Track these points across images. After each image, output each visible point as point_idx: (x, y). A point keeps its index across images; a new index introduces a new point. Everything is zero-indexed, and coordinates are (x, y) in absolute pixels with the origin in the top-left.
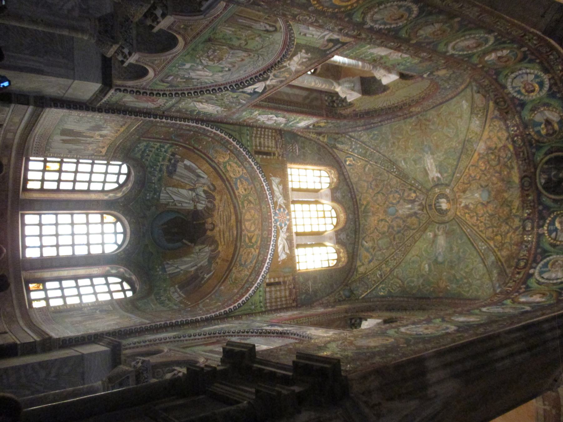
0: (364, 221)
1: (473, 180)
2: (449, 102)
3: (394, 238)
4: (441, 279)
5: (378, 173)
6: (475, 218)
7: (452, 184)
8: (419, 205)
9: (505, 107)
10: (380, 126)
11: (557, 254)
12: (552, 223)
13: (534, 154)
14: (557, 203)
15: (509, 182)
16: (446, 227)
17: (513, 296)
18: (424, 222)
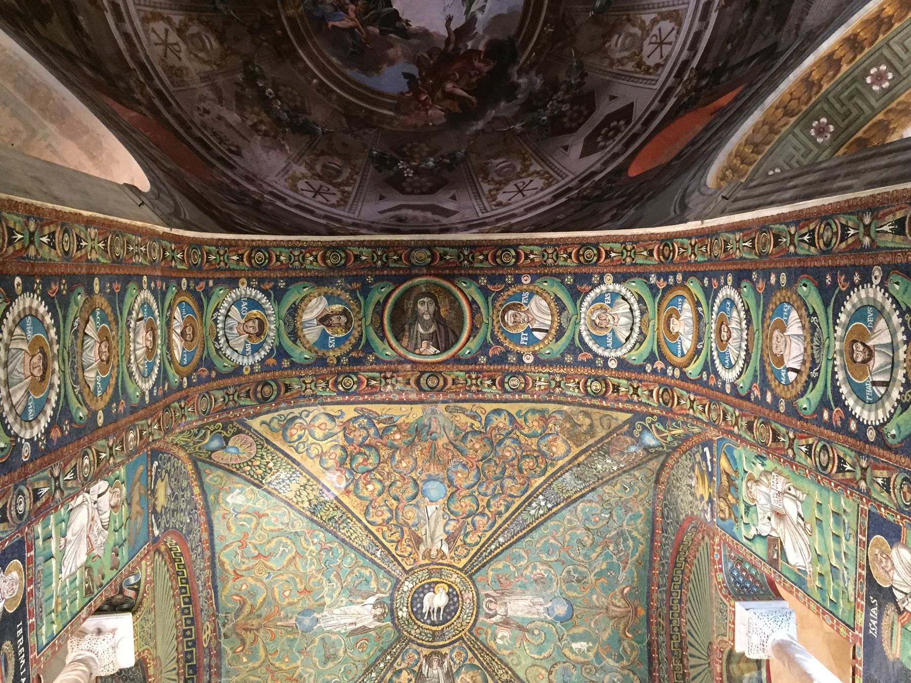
1: (397, 518)
2: (216, 541)
4: (607, 609)
6: (477, 518)
7: (397, 572)
9: (273, 383)
11: (577, 324)
12: (516, 338)
13: (378, 360)
14: (477, 329)
18: (470, 655)
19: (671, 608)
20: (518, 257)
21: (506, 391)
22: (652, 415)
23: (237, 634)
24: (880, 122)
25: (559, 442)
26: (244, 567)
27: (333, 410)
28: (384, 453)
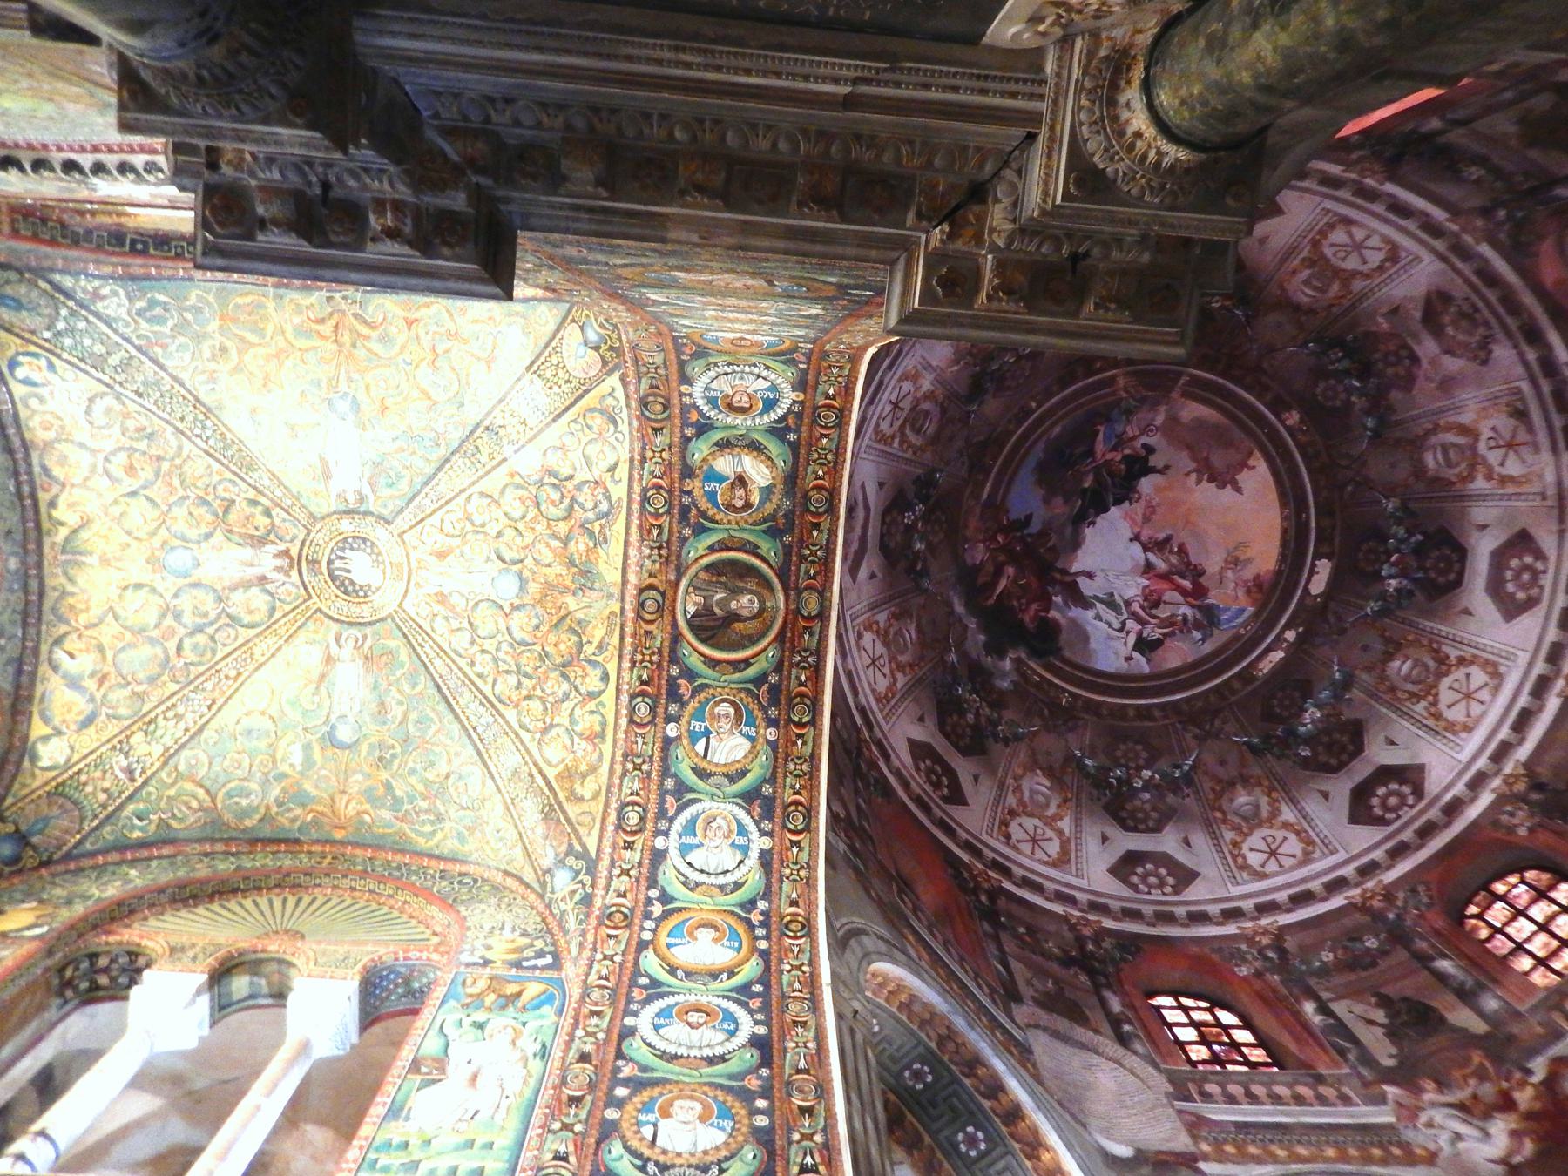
0: (62, 580)
3: (179, 648)
4: (344, 792)
5: (144, 429)
7: (402, 523)
8: (275, 556)
10: (183, 279)
11: (712, 797)
12: (698, 715)
13: (684, 540)
14: (713, 667)
15: (585, 573)
16: (365, 637)
17: (647, 936)
18: (288, 608)
19: (345, 876)
20: (800, 725)
21: (632, 697)
22: (593, 886)
23: (331, 314)
24: (921, 1140)
25: (564, 754)
26: (421, 332)
27: (623, 472)
28: (562, 527)
